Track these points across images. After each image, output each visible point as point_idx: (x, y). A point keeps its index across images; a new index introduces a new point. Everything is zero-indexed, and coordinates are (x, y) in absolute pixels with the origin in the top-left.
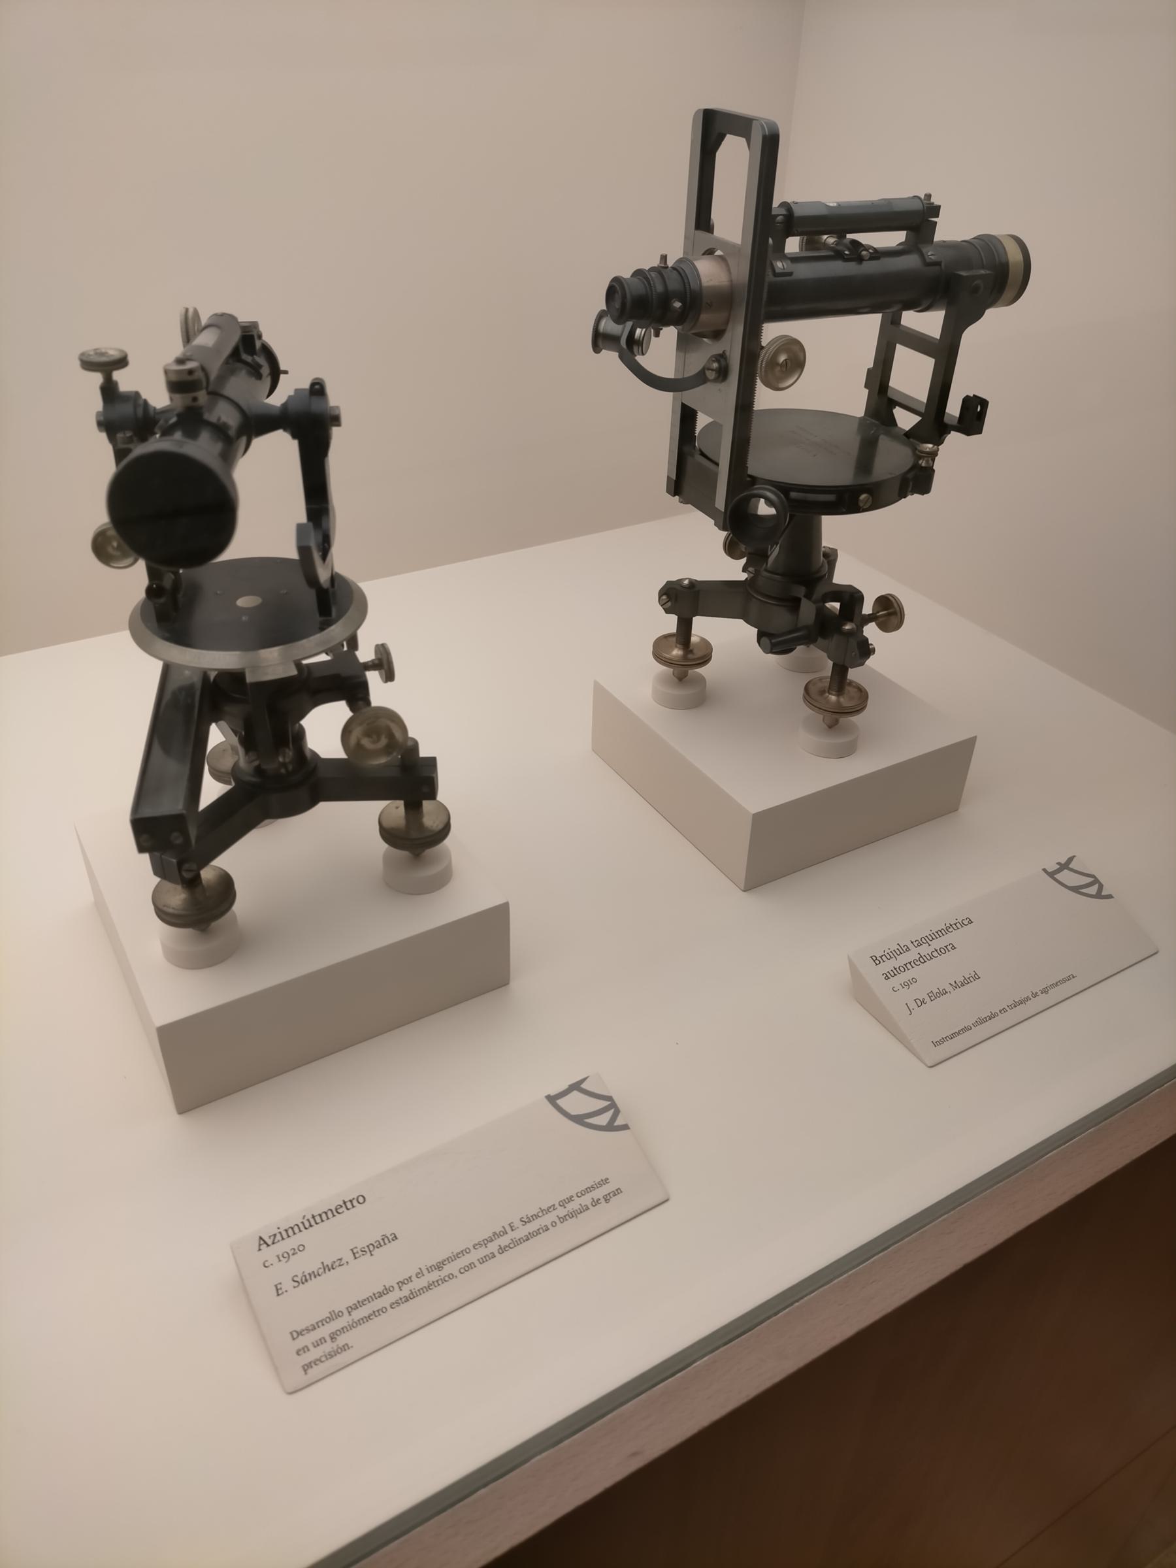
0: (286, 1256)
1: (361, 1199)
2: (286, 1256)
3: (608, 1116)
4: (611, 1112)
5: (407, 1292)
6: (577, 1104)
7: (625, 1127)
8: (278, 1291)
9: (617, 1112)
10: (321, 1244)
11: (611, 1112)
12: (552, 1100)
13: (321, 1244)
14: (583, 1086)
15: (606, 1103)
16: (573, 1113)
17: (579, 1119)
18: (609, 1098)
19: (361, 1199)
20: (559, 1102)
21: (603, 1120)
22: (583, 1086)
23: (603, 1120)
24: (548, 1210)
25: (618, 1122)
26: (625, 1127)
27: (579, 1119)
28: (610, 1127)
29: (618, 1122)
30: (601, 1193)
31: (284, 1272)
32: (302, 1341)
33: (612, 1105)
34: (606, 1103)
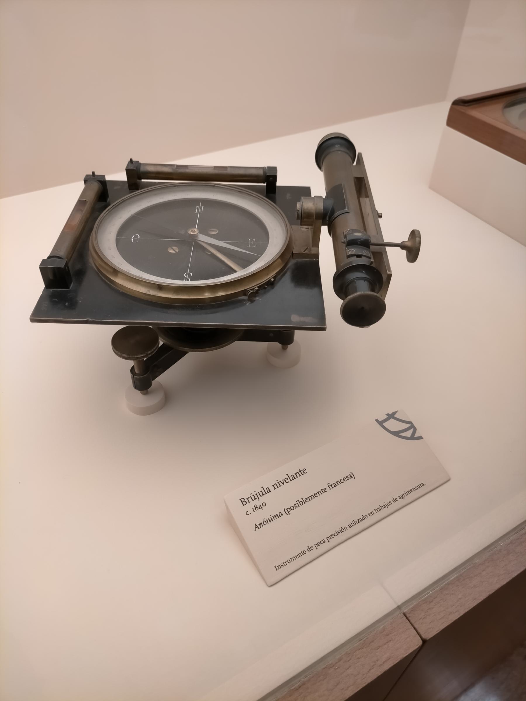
3: (410, 432)
4: (411, 431)
6: (393, 425)
7: (420, 438)
9: (415, 430)
11: (411, 431)
13: (275, 502)
14: (396, 416)
15: (409, 425)
16: (392, 430)
17: (396, 434)
20: (384, 424)
21: (408, 434)
22: (396, 416)
23: (408, 434)
25: (417, 435)
26: (420, 438)
27: (396, 434)
28: (413, 438)
29: (417, 435)
33: (412, 426)
34: (410, 425)
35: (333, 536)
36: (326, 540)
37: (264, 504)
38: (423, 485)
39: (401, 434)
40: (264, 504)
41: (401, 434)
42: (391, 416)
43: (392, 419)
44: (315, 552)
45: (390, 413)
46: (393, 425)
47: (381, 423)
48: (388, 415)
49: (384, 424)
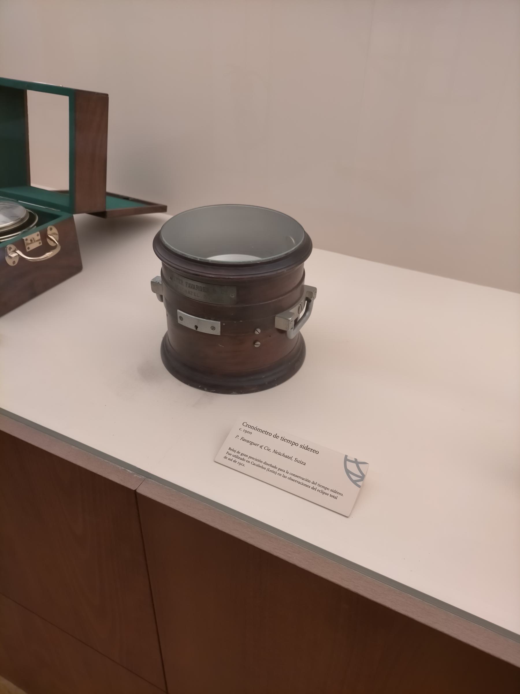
0: (246, 432)
1: (317, 452)
2: (246, 432)
3: (358, 479)
5: (294, 478)
6: (352, 467)
7: (359, 486)
8: (238, 436)
10: (255, 437)
12: (346, 459)
13: (255, 437)
14: (360, 465)
15: (361, 475)
16: (348, 468)
17: (348, 472)
19: (317, 452)
20: (347, 462)
22: (360, 465)
23: (354, 478)
24: (233, 450)
25: (360, 483)
26: (359, 486)
27: (348, 472)
28: (355, 482)
29: (360, 483)
30: (335, 494)
31: (242, 434)
32: (230, 452)
33: (362, 477)
34: (361, 475)
37: (251, 433)
39: (350, 475)
40: (251, 433)
41: (350, 475)
42: (356, 462)
46: (352, 467)
47: (346, 459)
48: (356, 459)
49: (347, 462)
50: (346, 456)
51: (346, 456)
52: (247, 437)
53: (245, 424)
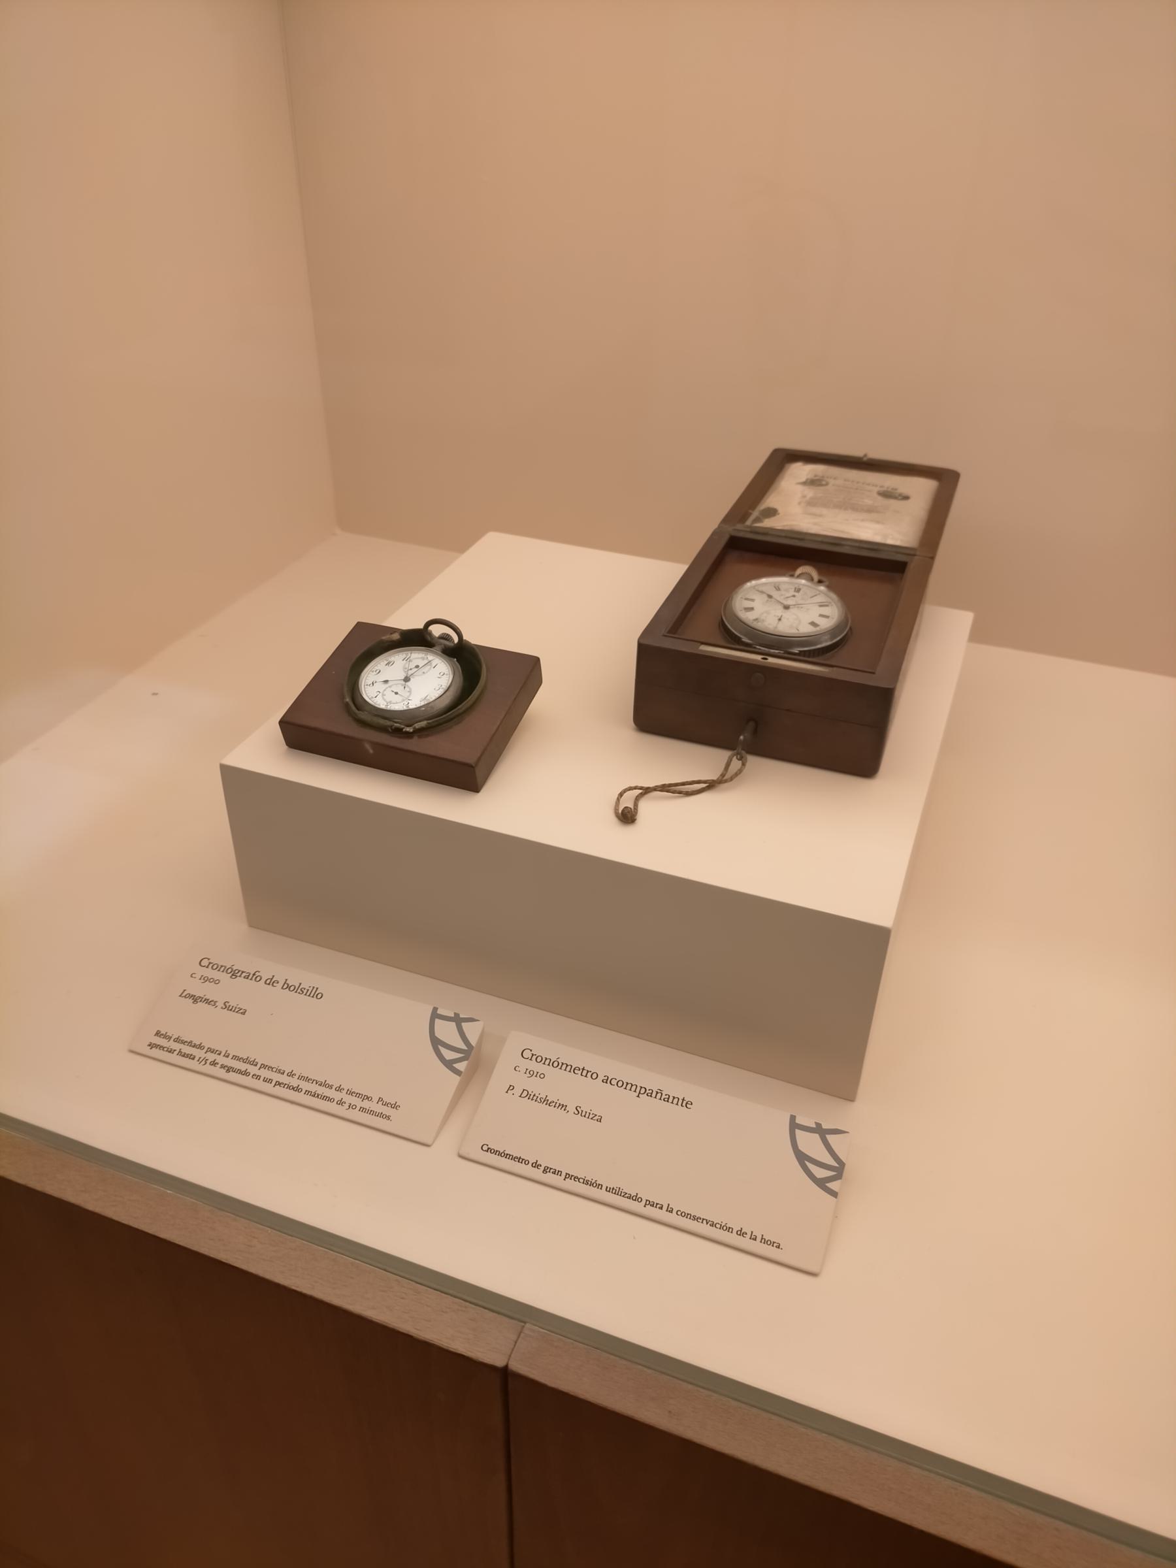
0: (531, 1074)
6: (810, 1144)
7: (834, 1194)
8: (511, 1088)
14: (828, 1137)
15: (833, 1163)
16: (802, 1147)
17: (802, 1158)
18: (842, 1164)
20: (798, 1131)
22: (828, 1137)
25: (833, 1185)
26: (834, 1194)
27: (802, 1158)
28: (821, 1183)
29: (833, 1185)
31: (523, 1082)
33: (839, 1170)
34: (833, 1163)
35: (576, 1178)
36: (564, 1175)
38: (778, 1247)
42: (819, 1130)
43: (816, 1137)
44: (537, 1174)
45: (824, 1127)
46: (810, 1144)
49: (798, 1131)
50: (793, 1118)
51: (793, 1118)
52: (534, 1086)
53: (527, 1054)
